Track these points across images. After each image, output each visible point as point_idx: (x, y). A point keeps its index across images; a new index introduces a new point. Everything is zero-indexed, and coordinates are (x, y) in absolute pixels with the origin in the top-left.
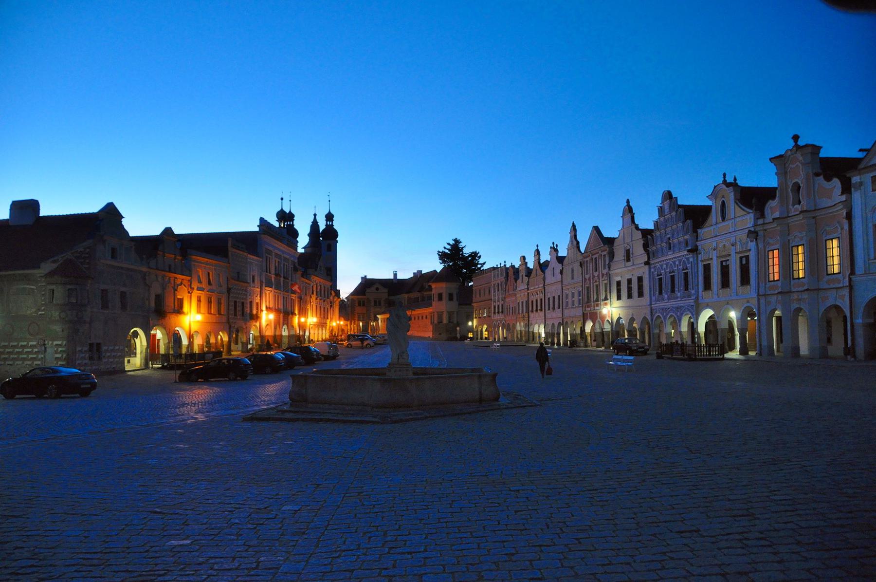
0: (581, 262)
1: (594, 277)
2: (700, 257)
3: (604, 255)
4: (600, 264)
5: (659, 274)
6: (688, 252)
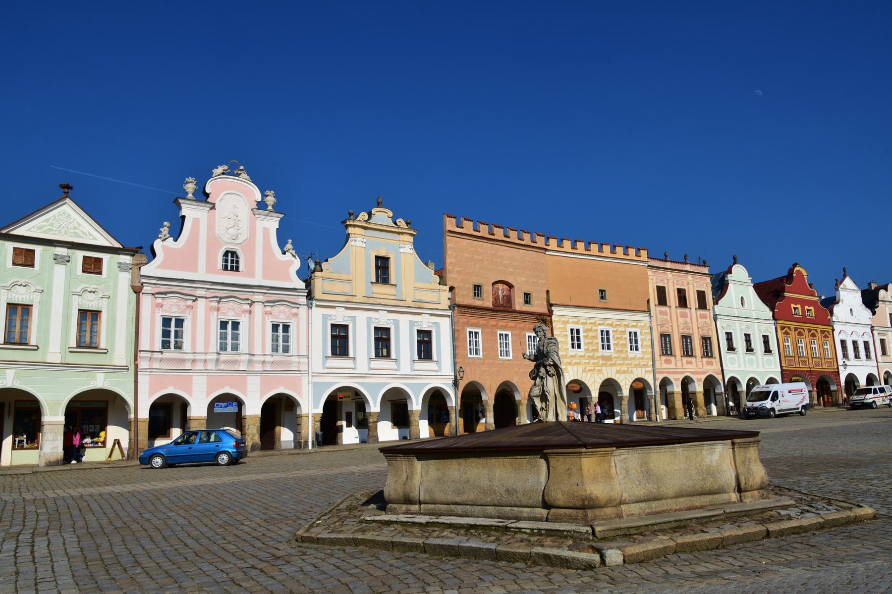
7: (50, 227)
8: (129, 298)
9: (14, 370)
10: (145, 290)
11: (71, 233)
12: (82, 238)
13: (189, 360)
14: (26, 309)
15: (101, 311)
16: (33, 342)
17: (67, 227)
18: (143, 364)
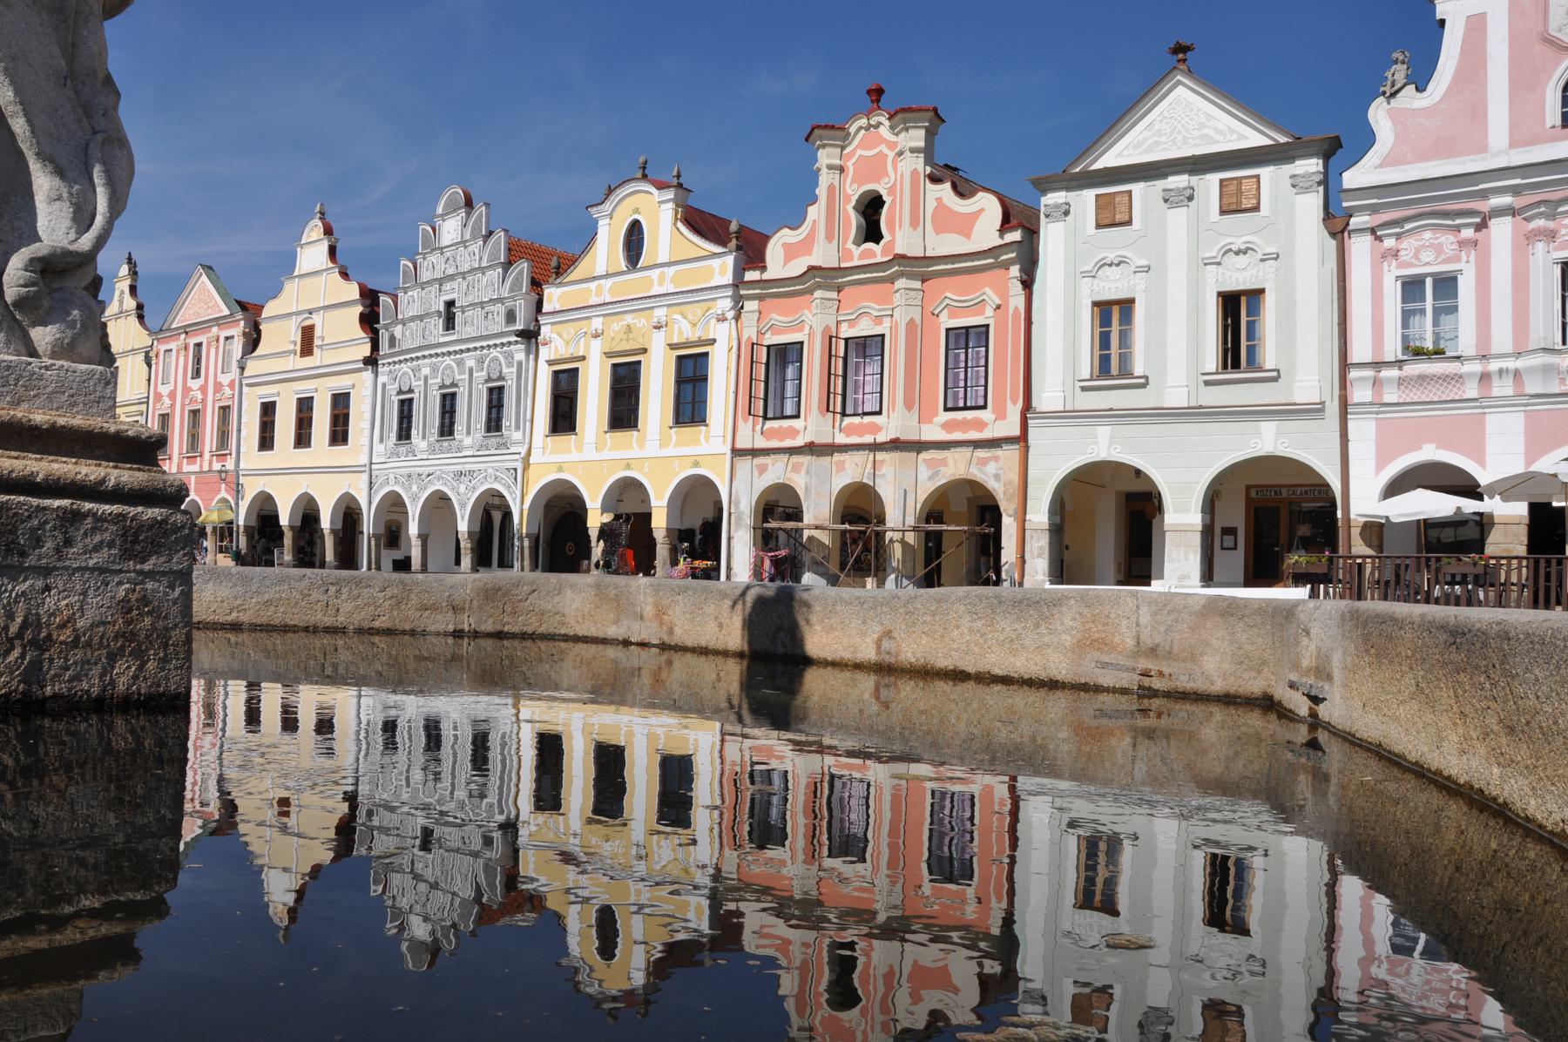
0: (147, 353)
1: (186, 390)
2: (545, 354)
3: (227, 338)
4: (211, 358)
5: (405, 388)
6: (517, 336)
7: (1156, 138)
8: (1322, 249)
9: (1110, 427)
10: (1355, 224)
11: (1194, 139)
12: (1219, 142)
13: (1470, 375)
14: (1127, 305)
15: (1262, 291)
16: (1138, 371)
17: (1187, 130)
18: (1360, 394)
